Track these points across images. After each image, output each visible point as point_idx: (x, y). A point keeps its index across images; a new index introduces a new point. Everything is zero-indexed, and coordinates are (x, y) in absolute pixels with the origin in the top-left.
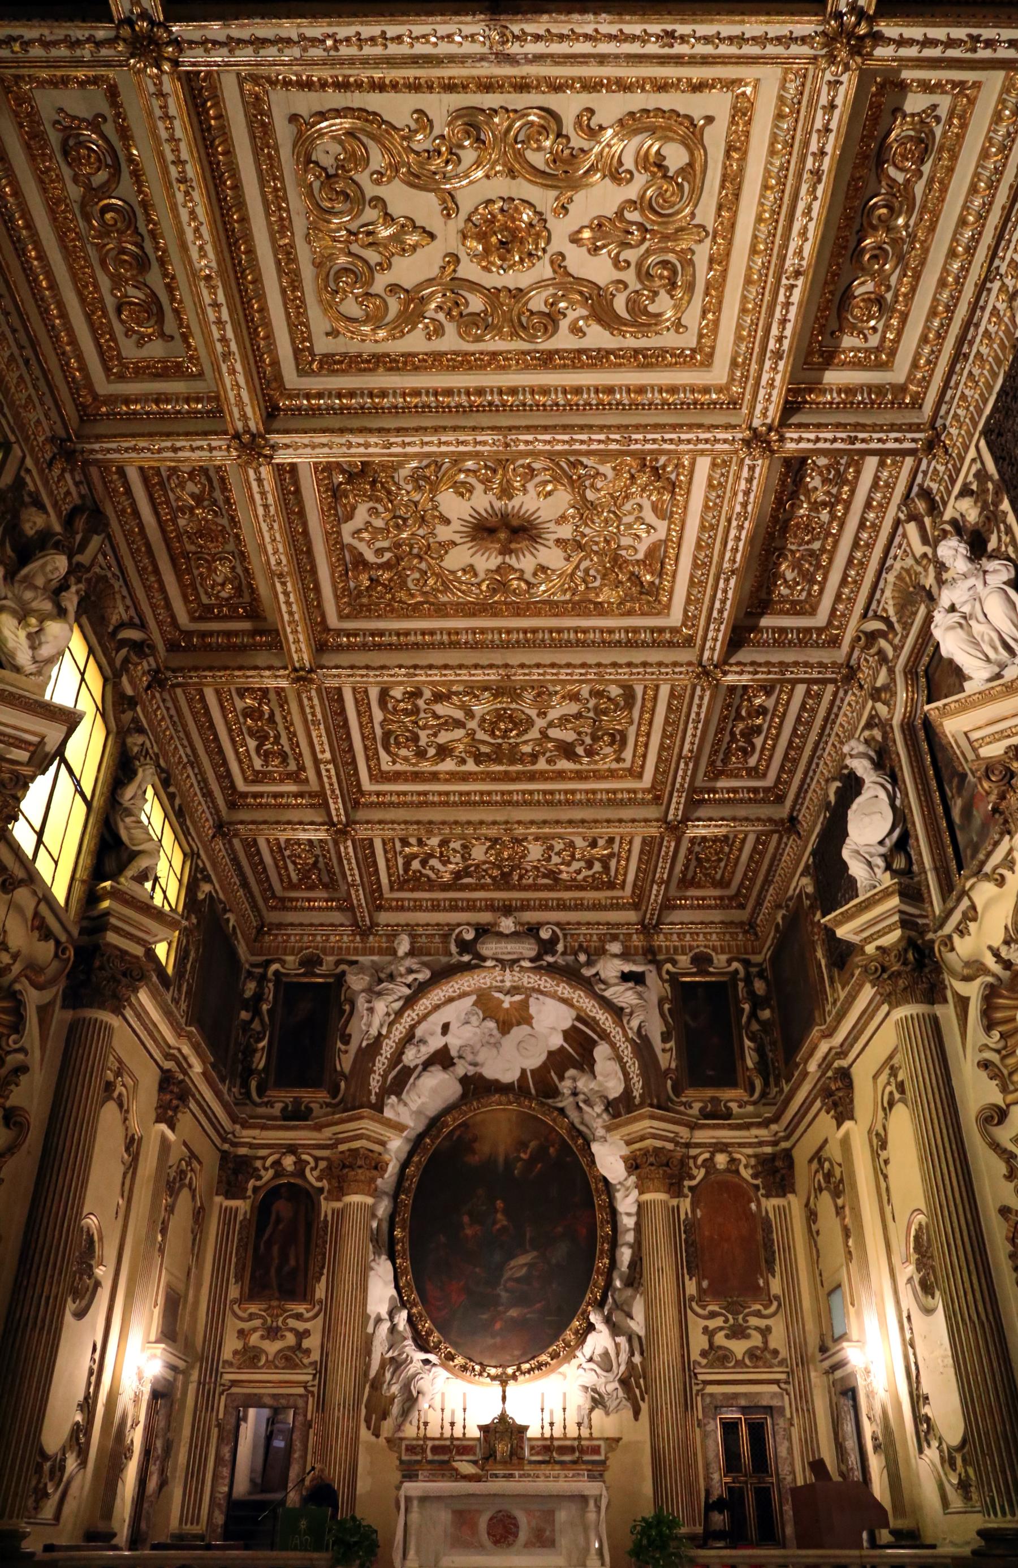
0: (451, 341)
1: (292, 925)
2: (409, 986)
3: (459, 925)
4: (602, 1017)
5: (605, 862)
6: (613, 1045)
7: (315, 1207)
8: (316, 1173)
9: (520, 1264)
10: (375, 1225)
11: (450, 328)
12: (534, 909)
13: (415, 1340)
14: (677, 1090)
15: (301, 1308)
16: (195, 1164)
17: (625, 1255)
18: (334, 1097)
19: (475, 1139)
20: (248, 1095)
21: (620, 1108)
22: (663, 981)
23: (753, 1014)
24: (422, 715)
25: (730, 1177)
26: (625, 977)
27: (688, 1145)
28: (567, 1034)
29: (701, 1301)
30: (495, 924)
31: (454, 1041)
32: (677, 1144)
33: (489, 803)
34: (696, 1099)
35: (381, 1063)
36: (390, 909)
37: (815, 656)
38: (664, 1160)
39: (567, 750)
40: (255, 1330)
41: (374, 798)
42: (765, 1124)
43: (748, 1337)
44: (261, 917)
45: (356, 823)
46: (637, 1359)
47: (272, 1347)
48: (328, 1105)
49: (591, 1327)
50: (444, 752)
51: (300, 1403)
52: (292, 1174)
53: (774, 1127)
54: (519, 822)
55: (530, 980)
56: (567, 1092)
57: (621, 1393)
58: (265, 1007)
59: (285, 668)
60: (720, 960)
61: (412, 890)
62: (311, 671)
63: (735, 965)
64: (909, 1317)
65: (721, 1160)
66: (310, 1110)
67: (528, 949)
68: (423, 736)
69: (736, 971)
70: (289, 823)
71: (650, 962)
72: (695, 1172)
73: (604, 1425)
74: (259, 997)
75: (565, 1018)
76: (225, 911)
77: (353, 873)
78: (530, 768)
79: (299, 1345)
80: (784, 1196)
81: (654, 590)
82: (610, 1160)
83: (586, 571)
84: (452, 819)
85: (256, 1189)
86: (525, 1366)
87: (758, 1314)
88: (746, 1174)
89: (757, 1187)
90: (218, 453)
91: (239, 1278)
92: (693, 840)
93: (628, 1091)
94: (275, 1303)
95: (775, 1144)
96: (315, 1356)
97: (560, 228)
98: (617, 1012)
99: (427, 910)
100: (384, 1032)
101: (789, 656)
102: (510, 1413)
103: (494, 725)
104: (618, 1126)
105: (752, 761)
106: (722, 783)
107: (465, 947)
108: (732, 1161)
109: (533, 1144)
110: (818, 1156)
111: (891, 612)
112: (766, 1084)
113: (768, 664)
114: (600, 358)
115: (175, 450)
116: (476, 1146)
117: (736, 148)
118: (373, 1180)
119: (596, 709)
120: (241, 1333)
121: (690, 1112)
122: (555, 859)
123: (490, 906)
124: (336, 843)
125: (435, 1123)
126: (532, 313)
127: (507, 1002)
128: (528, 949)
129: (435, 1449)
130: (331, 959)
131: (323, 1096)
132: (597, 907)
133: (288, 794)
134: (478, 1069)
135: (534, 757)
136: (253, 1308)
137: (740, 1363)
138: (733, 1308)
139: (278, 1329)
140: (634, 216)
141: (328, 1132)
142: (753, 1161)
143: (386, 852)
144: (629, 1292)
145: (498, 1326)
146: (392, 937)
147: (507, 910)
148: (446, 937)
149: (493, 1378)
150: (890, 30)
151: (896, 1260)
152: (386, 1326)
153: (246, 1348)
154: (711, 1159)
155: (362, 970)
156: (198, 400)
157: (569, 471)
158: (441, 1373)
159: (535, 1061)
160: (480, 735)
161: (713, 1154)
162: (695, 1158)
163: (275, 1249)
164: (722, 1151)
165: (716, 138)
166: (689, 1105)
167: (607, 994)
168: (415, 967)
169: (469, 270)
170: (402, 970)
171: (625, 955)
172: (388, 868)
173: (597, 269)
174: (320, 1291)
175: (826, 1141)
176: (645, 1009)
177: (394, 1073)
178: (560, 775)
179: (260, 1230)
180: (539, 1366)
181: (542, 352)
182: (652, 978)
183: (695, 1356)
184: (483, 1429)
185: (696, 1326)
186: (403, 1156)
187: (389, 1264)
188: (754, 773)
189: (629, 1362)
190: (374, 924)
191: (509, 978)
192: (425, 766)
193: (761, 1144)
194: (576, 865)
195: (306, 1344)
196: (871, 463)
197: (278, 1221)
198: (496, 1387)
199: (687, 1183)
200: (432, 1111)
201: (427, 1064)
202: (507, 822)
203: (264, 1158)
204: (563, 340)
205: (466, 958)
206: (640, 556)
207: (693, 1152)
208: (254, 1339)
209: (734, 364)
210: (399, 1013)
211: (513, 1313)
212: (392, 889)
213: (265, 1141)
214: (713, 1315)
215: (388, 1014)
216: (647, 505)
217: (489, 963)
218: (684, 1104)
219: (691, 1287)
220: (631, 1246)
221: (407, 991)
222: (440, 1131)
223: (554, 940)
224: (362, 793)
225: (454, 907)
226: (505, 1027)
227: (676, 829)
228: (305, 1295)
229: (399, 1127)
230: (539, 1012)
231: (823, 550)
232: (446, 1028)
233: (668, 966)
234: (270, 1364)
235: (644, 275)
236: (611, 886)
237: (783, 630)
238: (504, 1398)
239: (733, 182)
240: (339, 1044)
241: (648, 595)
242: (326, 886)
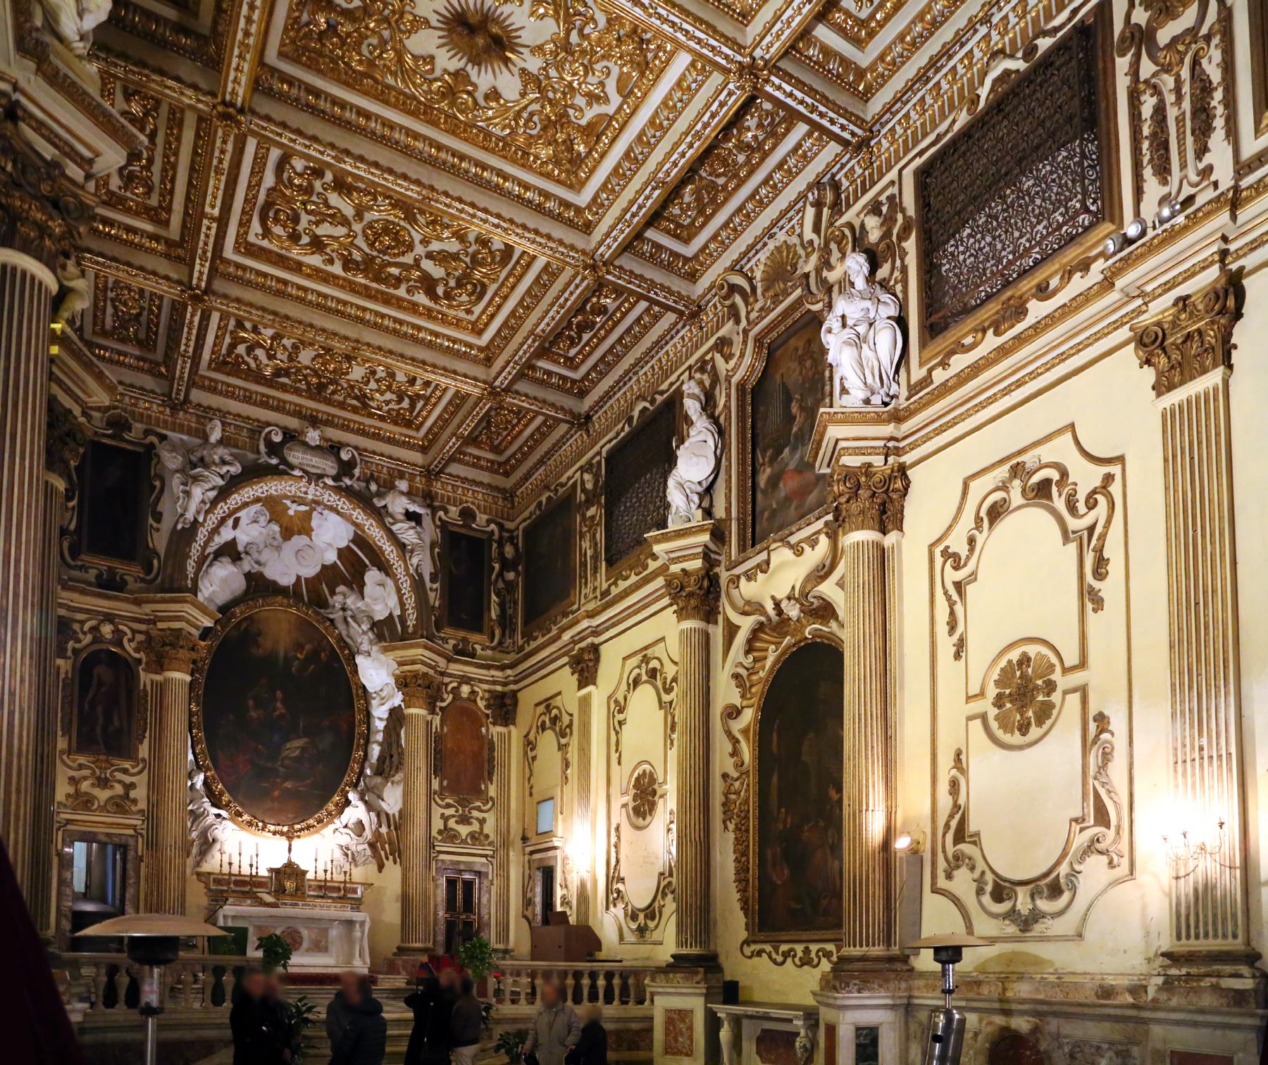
5: (413, 400)
22: (436, 527)
23: (500, 574)
24: (314, 198)
27: (443, 674)
28: (341, 553)
34: (452, 637)
38: (427, 683)
39: (428, 284)
42: (502, 668)
50: (317, 244)
53: (509, 672)
54: (369, 345)
63: (493, 526)
65: (465, 690)
68: (305, 219)
69: (493, 531)
72: (445, 696)
78: (391, 291)
82: (376, 673)
95: (505, 684)
96: (142, 805)
106: (541, 364)
108: (473, 692)
109: (308, 647)
110: (547, 703)
112: (503, 635)
116: (260, 639)
121: (446, 646)
122: (373, 385)
127: (293, 509)
135: (398, 281)
151: (615, 790)
160: (360, 242)
161: (460, 684)
164: (467, 683)
166: (445, 640)
175: (559, 693)
188: (571, 363)
192: (295, 253)
199: (439, 704)
202: (357, 341)
207: (447, 680)
218: (442, 639)
230: (320, 526)
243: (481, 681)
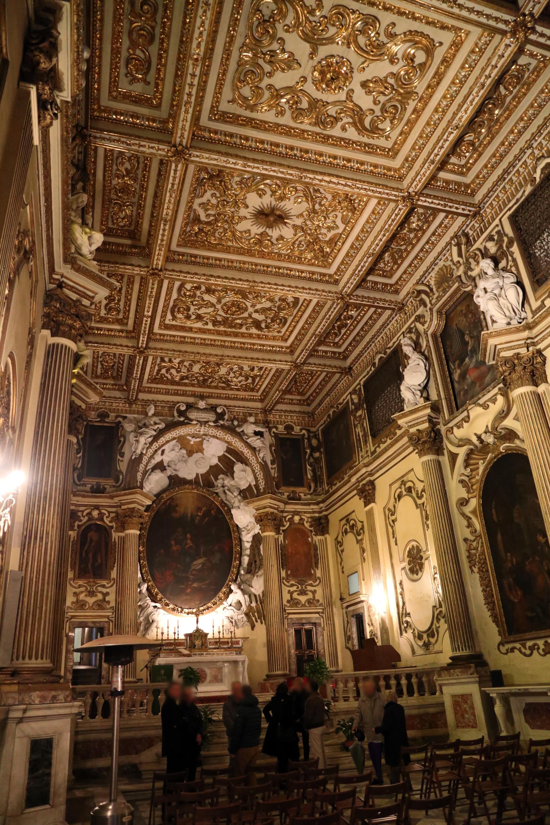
0: (286, 120)
7: (109, 535)
8: (109, 519)
9: (198, 563)
11: (288, 113)
15: (104, 583)
18: (117, 482)
23: (311, 455)
25: (301, 527)
26: (256, 433)
27: (282, 512)
29: (287, 580)
30: (196, 403)
31: (166, 459)
33: (214, 345)
34: (286, 491)
36: (145, 392)
37: (389, 297)
42: (318, 503)
43: (306, 594)
47: (91, 600)
48: (114, 486)
51: (106, 625)
52: (97, 519)
59: (148, 267)
60: (297, 429)
62: (161, 270)
63: (304, 431)
64: (401, 583)
65: (297, 518)
66: (105, 489)
67: (211, 417)
70: (115, 345)
73: (239, 633)
79: (104, 599)
80: (323, 535)
81: (326, 256)
83: (300, 242)
85: (79, 526)
87: (311, 585)
88: (307, 525)
89: (311, 531)
90: (158, 150)
91: (73, 568)
94: (91, 580)
97: (358, 78)
99: (162, 394)
101: (378, 295)
102: (200, 627)
103: (229, 308)
105: (337, 340)
107: (181, 413)
111: (432, 283)
112: (316, 486)
113: (369, 298)
114: (348, 143)
115: (141, 146)
117: (446, 62)
119: (279, 307)
120: (75, 594)
123: (194, 395)
126: (328, 116)
128: (211, 417)
130: (113, 415)
131: (111, 482)
133: (115, 330)
136: (81, 582)
137: (304, 605)
138: (301, 582)
139: (93, 592)
140: (391, 81)
141: (116, 500)
144: (249, 576)
145: (189, 590)
147: (202, 397)
148: (171, 408)
150: (539, 29)
154: (292, 518)
155: (130, 421)
156: (154, 121)
157: (311, 194)
158: (161, 611)
159: (203, 470)
161: (293, 516)
163: (90, 555)
165: (439, 54)
166: (282, 494)
167: (248, 441)
168: (158, 421)
169: (309, 87)
171: (256, 423)
173: (364, 101)
178: (250, 336)
179: (83, 544)
180: (208, 608)
181: (325, 135)
182: (266, 435)
183: (285, 602)
185: (285, 589)
190: (137, 399)
193: (314, 512)
195: (107, 598)
196: (442, 215)
197: (91, 541)
198: (194, 617)
203: (83, 511)
204: (336, 131)
205: (182, 419)
206: (327, 239)
207: (285, 515)
208: (82, 597)
209: (406, 160)
210: (151, 443)
211: (195, 585)
214: (292, 585)
216: (340, 215)
217: (194, 422)
219: (283, 574)
220: (249, 556)
221: (154, 433)
225: (176, 393)
231: (406, 250)
233: (274, 430)
234: (91, 608)
235: (384, 110)
237: (376, 283)
238: (197, 622)
239: (439, 76)
240: (119, 457)
241: (324, 258)
243: (305, 512)
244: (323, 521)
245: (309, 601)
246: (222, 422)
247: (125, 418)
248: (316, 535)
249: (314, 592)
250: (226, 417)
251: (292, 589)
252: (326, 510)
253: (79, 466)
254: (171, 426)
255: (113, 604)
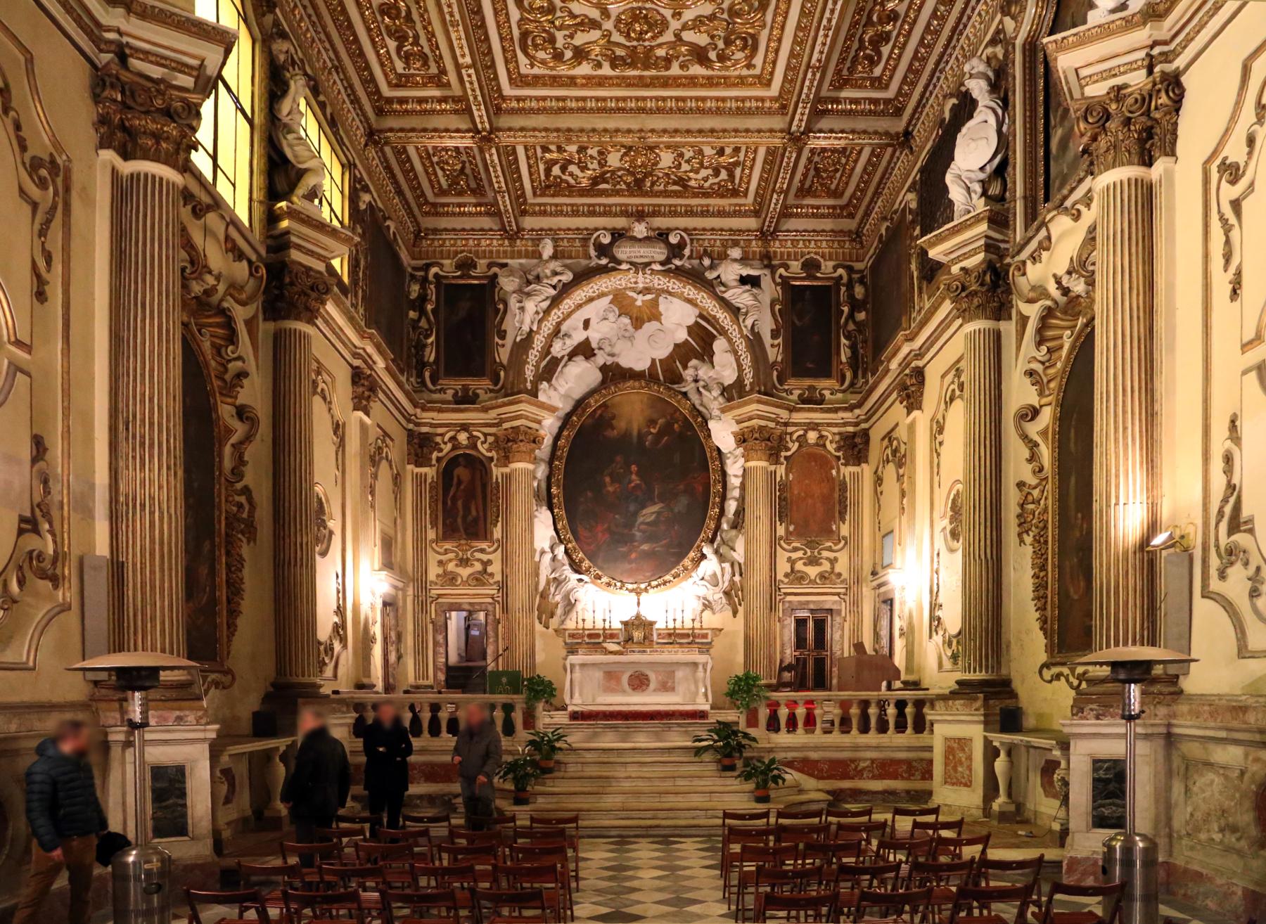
1: (446, 230)
2: (554, 287)
3: (597, 230)
4: (723, 317)
6: (730, 340)
8: (486, 446)
10: (535, 484)
12: (664, 215)
13: (571, 566)
14: (781, 380)
15: (484, 545)
16: (388, 440)
17: (731, 506)
19: (614, 417)
20: (423, 383)
21: (734, 392)
26: (744, 280)
27: (786, 424)
32: (778, 423)
34: (796, 387)
35: (533, 356)
36: (534, 214)
40: (451, 560)
41: (514, 104)
42: (851, 408)
43: (820, 564)
44: (418, 224)
45: (499, 130)
46: (737, 578)
48: (491, 391)
49: (703, 557)
51: (490, 608)
52: (467, 447)
53: (857, 412)
55: (660, 282)
56: (689, 379)
57: (724, 601)
58: (429, 307)
60: (827, 266)
61: (553, 196)
67: (659, 253)
71: (766, 267)
72: (790, 445)
74: (423, 298)
75: (689, 315)
76: (385, 219)
77: (499, 181)
79: (485, 570)
82: (723, 433)
84: (588, 126)
86: (654, 583)
89: (838, 458)
91: (434, 524)
92: (812, 151)
93: (740, 381)
98: (735, 311)
100: (535, 328)
104: (731, 408)
107: (603, 250)
108: (821, 437)
112: (855, 376)
118: (533, 451)
124: (481, 151)
125: (580, 404)
128: (659, 253)
129: (590, 636)
132: (721, 214)
134: (615, 359)
136: (448, 546)
137: (813, 582)
138: (811, 545)
139: (468, 559)
141: (493, 414)
142: (837, 438)
143: (528, 158)
146: (537, 241)
147: (640, 215)
148: (585, 241)
149: (631, 591)
152: (549, 556)
153: (445, 573)
154: (804, 435)
161: (806, 431)
162: (791, 434)
163: (460, 503)
164: (814, 429)
167: (726, 295)
168: (559, 269)
170: (548, 272)
171: (744, 260)
172: (531, 174)
174: (497, 533)
176: (759, 310)
177: (544, 363)
182: (766, 282)
183: (780, 576)
184: (625, 624)
185: (782, 556)
186: (555, 430)
187: (549, 513)
189: (732, 582)
190: (520, 229)
191: (642, 280)
193: (845, 424)
194: (704, 173)
195: (490, 569)
200: (577, 395)
201: (572, 355)
205: (604, 261)
207: (790, 429)
208: (451, 567)
212: (535, 194)
213: (442, 421)
214: (795, 549)
215: (537, 313)
219: (781, 531)
221: (553, 292)
222: (584, 411)
223: (681, 245)
224: (504, 99)
226: (638, 323)
227: (797, 140)
228: (485, 535)
229: (552, 409)
232: (587, 324)
236: (735, 193)
242: (474, 192)
243: (829, 425)
244: (858, 440)
245: (822, 576)
246: (677, 262)
247: (504, 265)
248: (845, 465)
249: (833, 562)
250: (687, 252)
251: (794, 555)
252: (866, 421)
253: (432, 359)
254: (583, 276)
255: (498, 577)
